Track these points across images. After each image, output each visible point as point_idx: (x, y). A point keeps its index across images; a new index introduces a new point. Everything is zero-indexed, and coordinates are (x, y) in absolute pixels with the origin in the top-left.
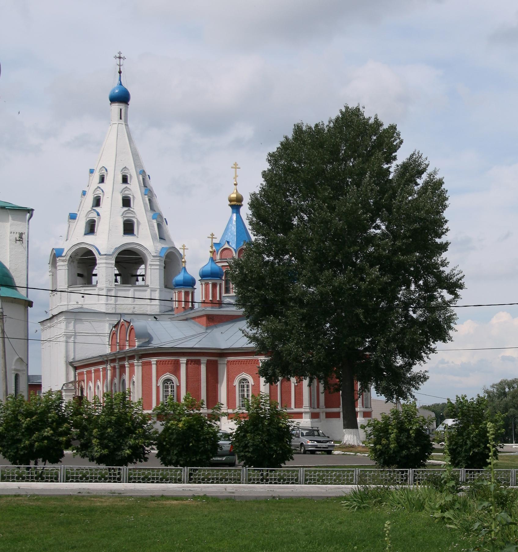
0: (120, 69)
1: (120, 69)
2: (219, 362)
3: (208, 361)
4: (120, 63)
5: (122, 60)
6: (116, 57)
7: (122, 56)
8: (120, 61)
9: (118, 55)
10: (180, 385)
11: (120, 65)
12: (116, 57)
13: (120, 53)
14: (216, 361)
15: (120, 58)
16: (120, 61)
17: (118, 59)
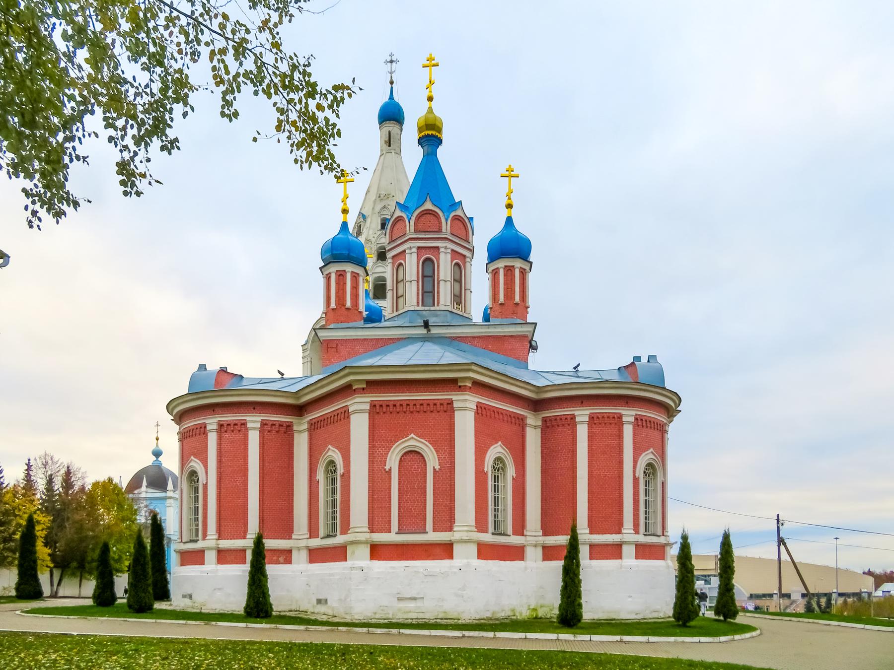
0: (391, 77)
1: (391, 77)
2: (295, 428)
3: (264, 424)
4: (391, 70)
5: (394, 63)
6: (386, 62)
7: (394, 59)
8: (391, 66)
9: (389, 59)
10: (207, 483)
11: (391, 73)
12: (386, 62)
13: (391, 55)
14: (289, 426)
15: (392, 62)
16: (391, 66)
17: (389, 64)
